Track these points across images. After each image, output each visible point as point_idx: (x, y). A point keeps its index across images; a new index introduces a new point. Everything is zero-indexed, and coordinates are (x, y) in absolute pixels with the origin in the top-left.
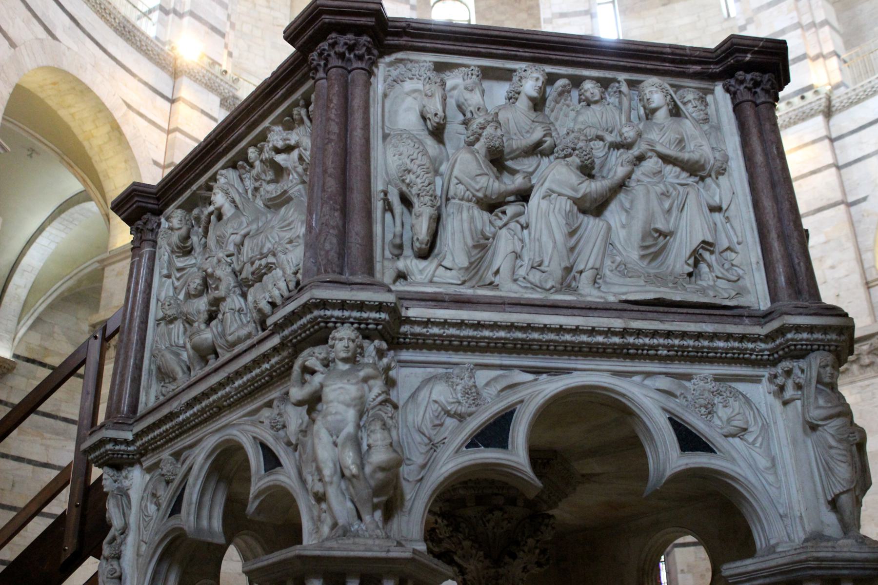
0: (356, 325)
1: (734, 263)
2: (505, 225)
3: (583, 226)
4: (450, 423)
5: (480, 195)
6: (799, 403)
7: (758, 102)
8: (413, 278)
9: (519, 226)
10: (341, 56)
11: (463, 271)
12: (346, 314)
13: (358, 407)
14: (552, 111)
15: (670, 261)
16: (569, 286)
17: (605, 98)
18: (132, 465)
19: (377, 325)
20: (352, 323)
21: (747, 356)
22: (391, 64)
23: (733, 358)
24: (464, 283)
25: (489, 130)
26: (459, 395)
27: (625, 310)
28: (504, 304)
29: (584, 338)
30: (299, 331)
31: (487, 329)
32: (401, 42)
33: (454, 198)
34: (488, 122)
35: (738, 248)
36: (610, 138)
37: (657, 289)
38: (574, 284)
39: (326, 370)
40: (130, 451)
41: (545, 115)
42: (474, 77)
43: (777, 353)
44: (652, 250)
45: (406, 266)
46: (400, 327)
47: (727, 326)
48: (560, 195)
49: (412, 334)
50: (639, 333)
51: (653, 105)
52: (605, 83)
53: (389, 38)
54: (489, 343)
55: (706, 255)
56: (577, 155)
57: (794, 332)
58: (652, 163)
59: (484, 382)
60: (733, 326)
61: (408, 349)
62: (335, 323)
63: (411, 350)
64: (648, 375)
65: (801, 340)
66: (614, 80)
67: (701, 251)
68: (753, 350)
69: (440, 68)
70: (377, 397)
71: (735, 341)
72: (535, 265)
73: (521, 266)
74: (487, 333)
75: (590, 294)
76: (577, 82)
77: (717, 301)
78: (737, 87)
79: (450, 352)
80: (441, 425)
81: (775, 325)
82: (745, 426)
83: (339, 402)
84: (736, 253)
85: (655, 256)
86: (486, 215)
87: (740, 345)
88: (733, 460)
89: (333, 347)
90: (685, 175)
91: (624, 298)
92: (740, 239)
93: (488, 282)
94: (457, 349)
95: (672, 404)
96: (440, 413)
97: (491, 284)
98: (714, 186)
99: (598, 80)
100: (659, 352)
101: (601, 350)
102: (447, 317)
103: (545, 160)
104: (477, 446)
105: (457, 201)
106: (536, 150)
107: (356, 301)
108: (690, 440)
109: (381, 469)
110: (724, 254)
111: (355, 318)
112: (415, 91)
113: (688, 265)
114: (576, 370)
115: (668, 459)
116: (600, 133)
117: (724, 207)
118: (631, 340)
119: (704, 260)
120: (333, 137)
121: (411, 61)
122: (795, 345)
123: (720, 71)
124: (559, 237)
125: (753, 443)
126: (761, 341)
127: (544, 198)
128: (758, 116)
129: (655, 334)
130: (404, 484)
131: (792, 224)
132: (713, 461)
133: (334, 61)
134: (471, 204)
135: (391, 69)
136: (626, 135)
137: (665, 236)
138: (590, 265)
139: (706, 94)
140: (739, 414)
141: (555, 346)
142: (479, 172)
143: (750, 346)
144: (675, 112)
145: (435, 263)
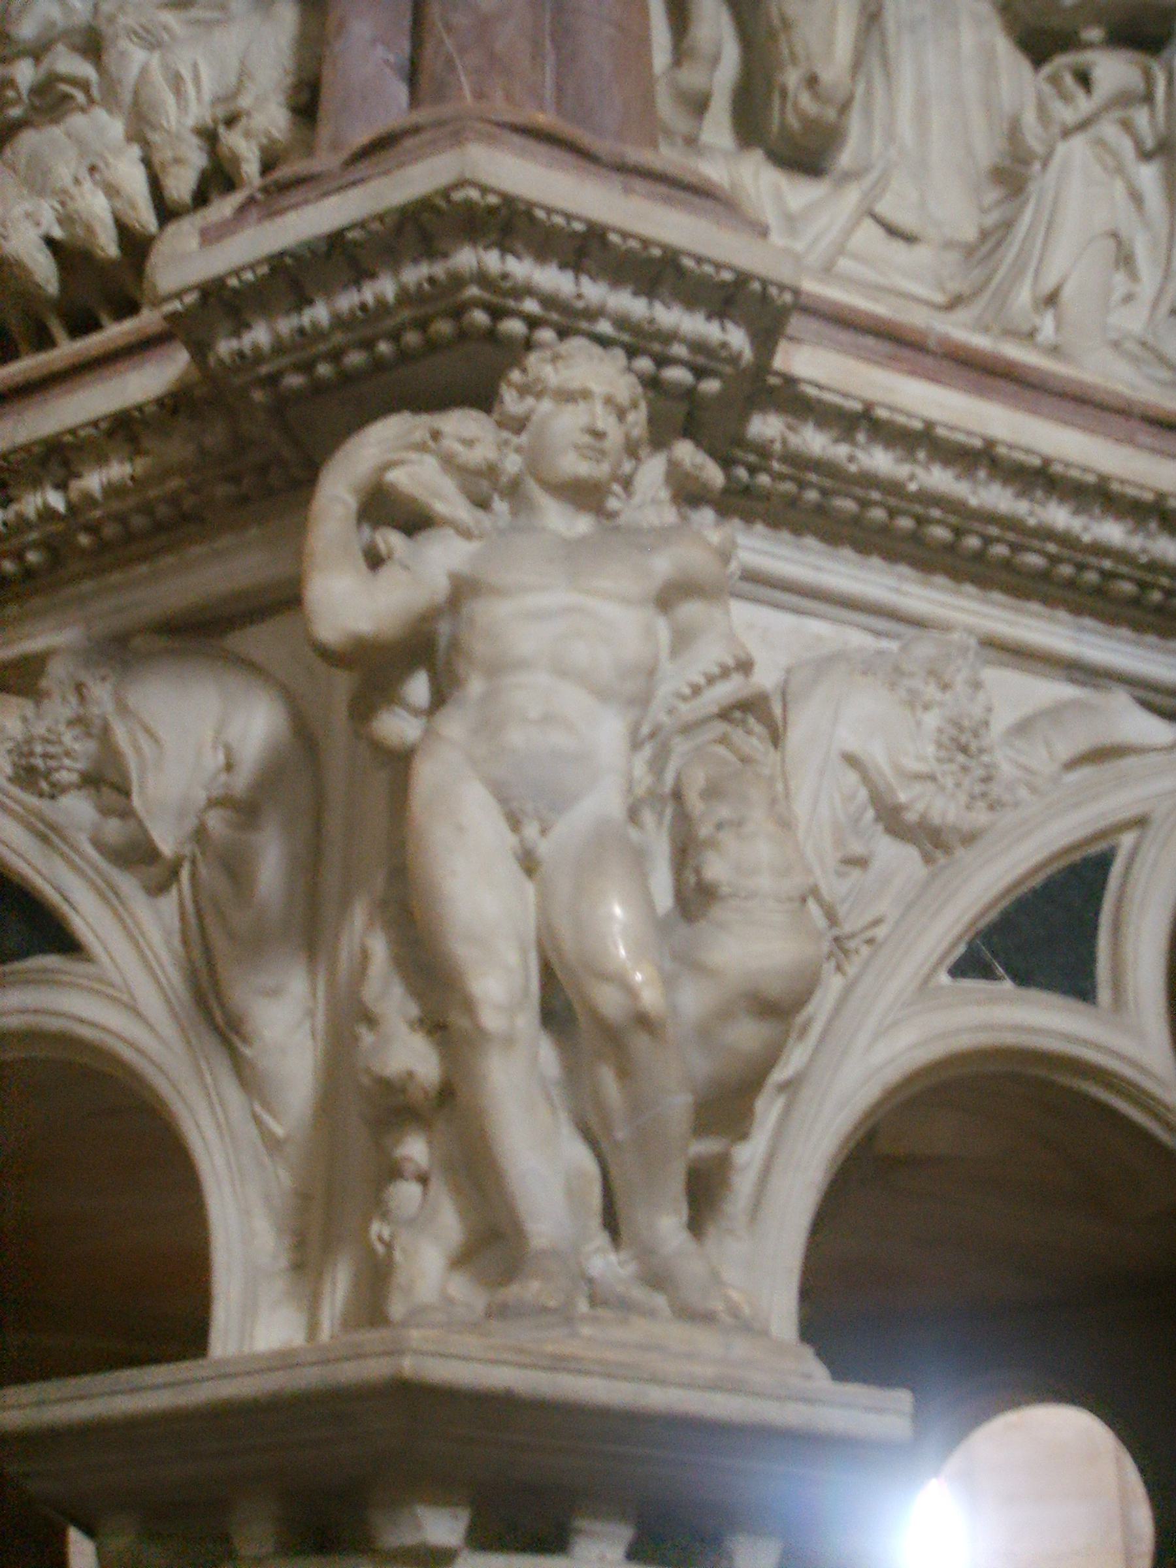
2: (1083, 125)
4: (896, 858)
9: (1127, 147)
11: (953, 257)
12: (594, 291)
19: (700, 373)
24: (954, 303)
30: (338, 338)
31: (1062, 499)
54: (1054, 560)
70: (711, 680)
73: (1128, 298)
79: (904, 569)
80: (860, 862)
83: (562, 671)
104: (986, 973)
107: (646, 243)
145: (852, 196)
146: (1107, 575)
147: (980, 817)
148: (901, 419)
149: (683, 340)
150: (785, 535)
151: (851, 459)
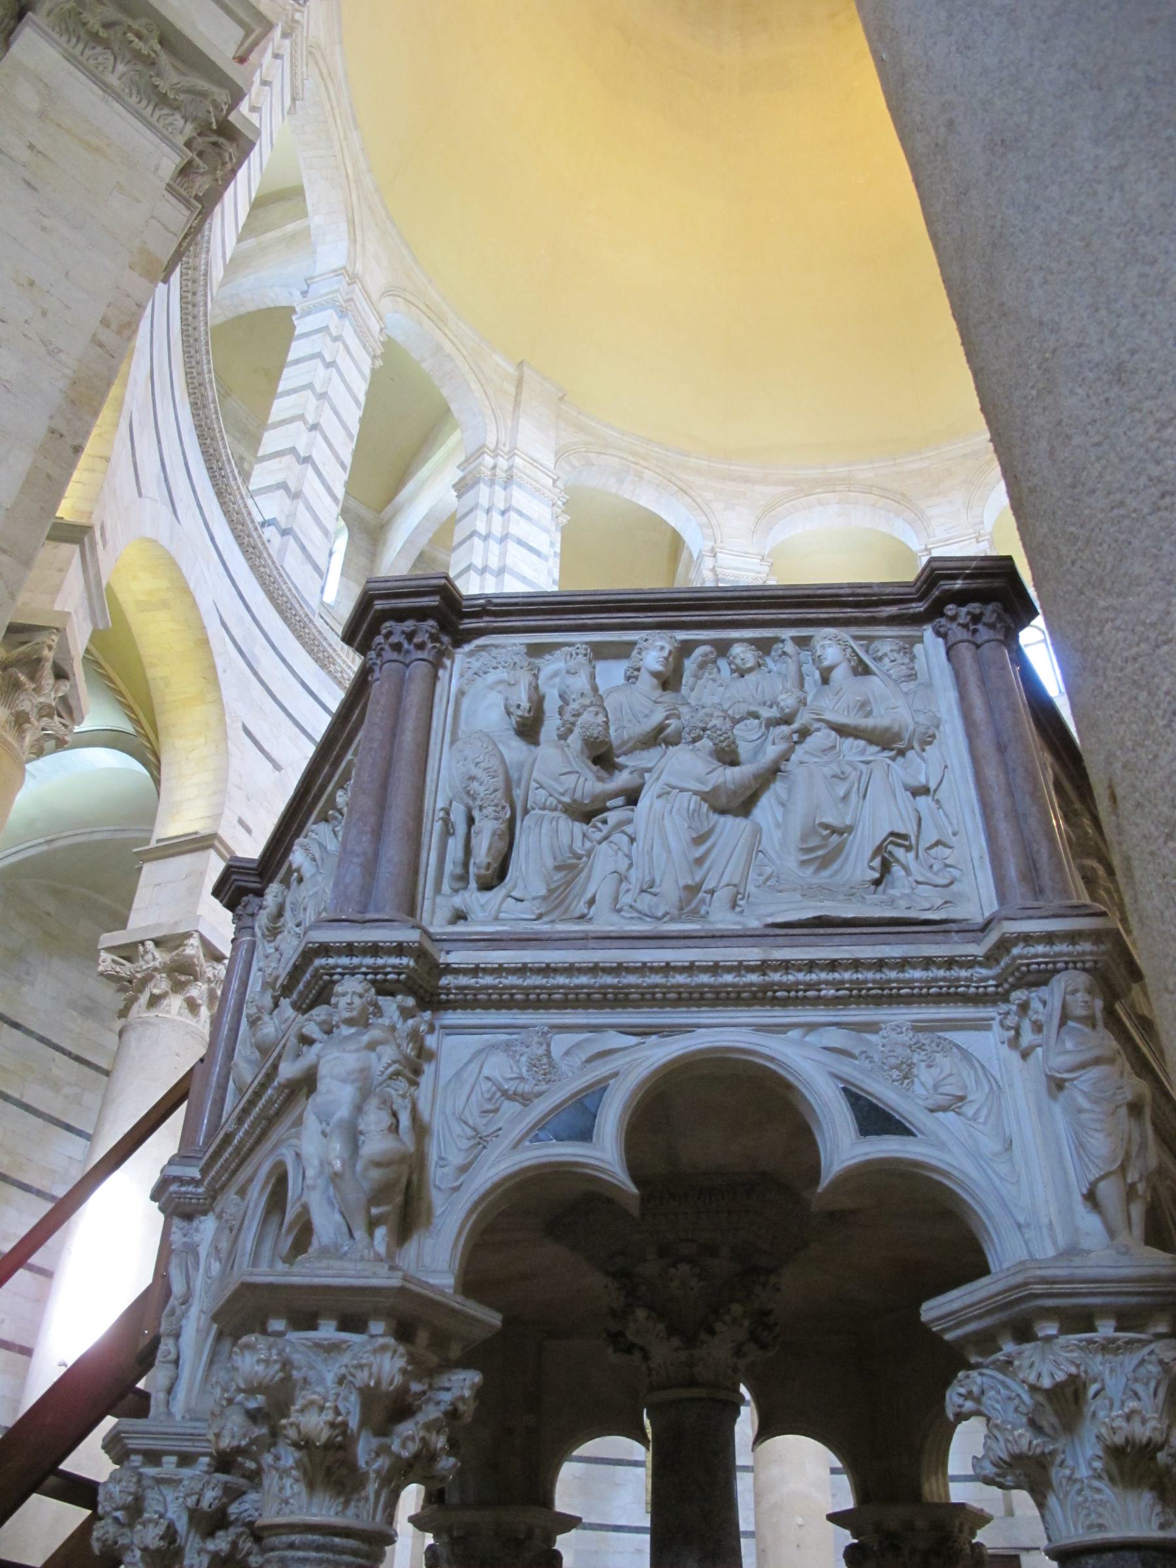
0: (370, 977)
2: (605, 838)
3: (718, 830)
4: (510, 1108)
5: (566, 799)
6: (1039, 1050)
7: (979, 642)
8: (473, 916)
9: (626, 838)
10: (397, 647)
12: (356, 961)
13: (358, 1084)
14: (692, 690)
15: (849, 867)
17: (765, 665)
18: (205, 1213)
19: (399, 974)
20: (366, 974)
21: (961, 990)
22: (471, 654)
23: (940, 995)
24: (540, 917)
25: (587, 717)
26: (524, 1070)
29: (705, 978)
33: (533, 809)
34: (585, 707)
35: (953, 841)
36: (766, 713)
39: (326, 1037)
40: (199, 1194)
41: (683, 697)
43: (1006, 980)
44: (820, 853)
45: (464, 901)
46: (439, 978)
47: (924, 947)
48: (682, 790)
49: (457, 988)
51: (826, 663)
52: (764, 647)
54: (566, 994)
55: (899, 853)
56: (708, 737)
57: (1021, 945)
58: (822, 737)
59: (564, 1050)
60: (934, 946)
61: (455, 1009)
62: (342, 975)
63: (459, 1011)
64: (811, 1027)
65: (1036, 956)
66: (777, 640)
67: (890, 847)
69: (536, 651)
71: (939, 968)
73: (628, 891)
74: (561, 980)
75: (722, 919)
76: (723, 648)
77: (912, 914)
78: (949, 626)
79: (515, 1011)
81: (993, 938)
82: (960, 1094)
85: (825, 863)
86: (578, 827)
88: (942, 1146)
89: (336, 1006)
90: (874, 749)
91: (770, 920)
92: (956, 828)
93: (578, 914)
95: (846, 1068)
96: (494, 1094)
97: (582, 917)
98: (918, 760)
100: (823, 993)
101: (733, 995)
105: (538, 812)
106: (657, 738)
107: (366, 942)
108: (874, 1118)
109: (378, 1164)
110: (932, 852)
111: (368, 967)
112: (500, 682)
113: (872, 868)
114: (699, 1026)
115: (843, 1148)
116: (752, 708)
117: (932, 786)
118: (776, 977)
119: (897, 861)
120: (375, 745)
121: (497, 646)
122: (1028, 965)
123: (926, 610)
125: (975, 1118)
126: (980, 964)
127: (659, 796)
128: (978, 660)
129: (811, 965)
130: (434, 1193)
131: (1027, 797)
132: (910, 1148)
133: (389, 654)
136: (782, 704)
137: (841, 833)
138: (724, 881)
139: (912, 645)
140: (950, 1075)
141: (664, 994)
142: (565, 770)
143: (964, 973)
144: (861, 669)
146: (589, 994)
147: (543, 1087)
150: (469, 1011)
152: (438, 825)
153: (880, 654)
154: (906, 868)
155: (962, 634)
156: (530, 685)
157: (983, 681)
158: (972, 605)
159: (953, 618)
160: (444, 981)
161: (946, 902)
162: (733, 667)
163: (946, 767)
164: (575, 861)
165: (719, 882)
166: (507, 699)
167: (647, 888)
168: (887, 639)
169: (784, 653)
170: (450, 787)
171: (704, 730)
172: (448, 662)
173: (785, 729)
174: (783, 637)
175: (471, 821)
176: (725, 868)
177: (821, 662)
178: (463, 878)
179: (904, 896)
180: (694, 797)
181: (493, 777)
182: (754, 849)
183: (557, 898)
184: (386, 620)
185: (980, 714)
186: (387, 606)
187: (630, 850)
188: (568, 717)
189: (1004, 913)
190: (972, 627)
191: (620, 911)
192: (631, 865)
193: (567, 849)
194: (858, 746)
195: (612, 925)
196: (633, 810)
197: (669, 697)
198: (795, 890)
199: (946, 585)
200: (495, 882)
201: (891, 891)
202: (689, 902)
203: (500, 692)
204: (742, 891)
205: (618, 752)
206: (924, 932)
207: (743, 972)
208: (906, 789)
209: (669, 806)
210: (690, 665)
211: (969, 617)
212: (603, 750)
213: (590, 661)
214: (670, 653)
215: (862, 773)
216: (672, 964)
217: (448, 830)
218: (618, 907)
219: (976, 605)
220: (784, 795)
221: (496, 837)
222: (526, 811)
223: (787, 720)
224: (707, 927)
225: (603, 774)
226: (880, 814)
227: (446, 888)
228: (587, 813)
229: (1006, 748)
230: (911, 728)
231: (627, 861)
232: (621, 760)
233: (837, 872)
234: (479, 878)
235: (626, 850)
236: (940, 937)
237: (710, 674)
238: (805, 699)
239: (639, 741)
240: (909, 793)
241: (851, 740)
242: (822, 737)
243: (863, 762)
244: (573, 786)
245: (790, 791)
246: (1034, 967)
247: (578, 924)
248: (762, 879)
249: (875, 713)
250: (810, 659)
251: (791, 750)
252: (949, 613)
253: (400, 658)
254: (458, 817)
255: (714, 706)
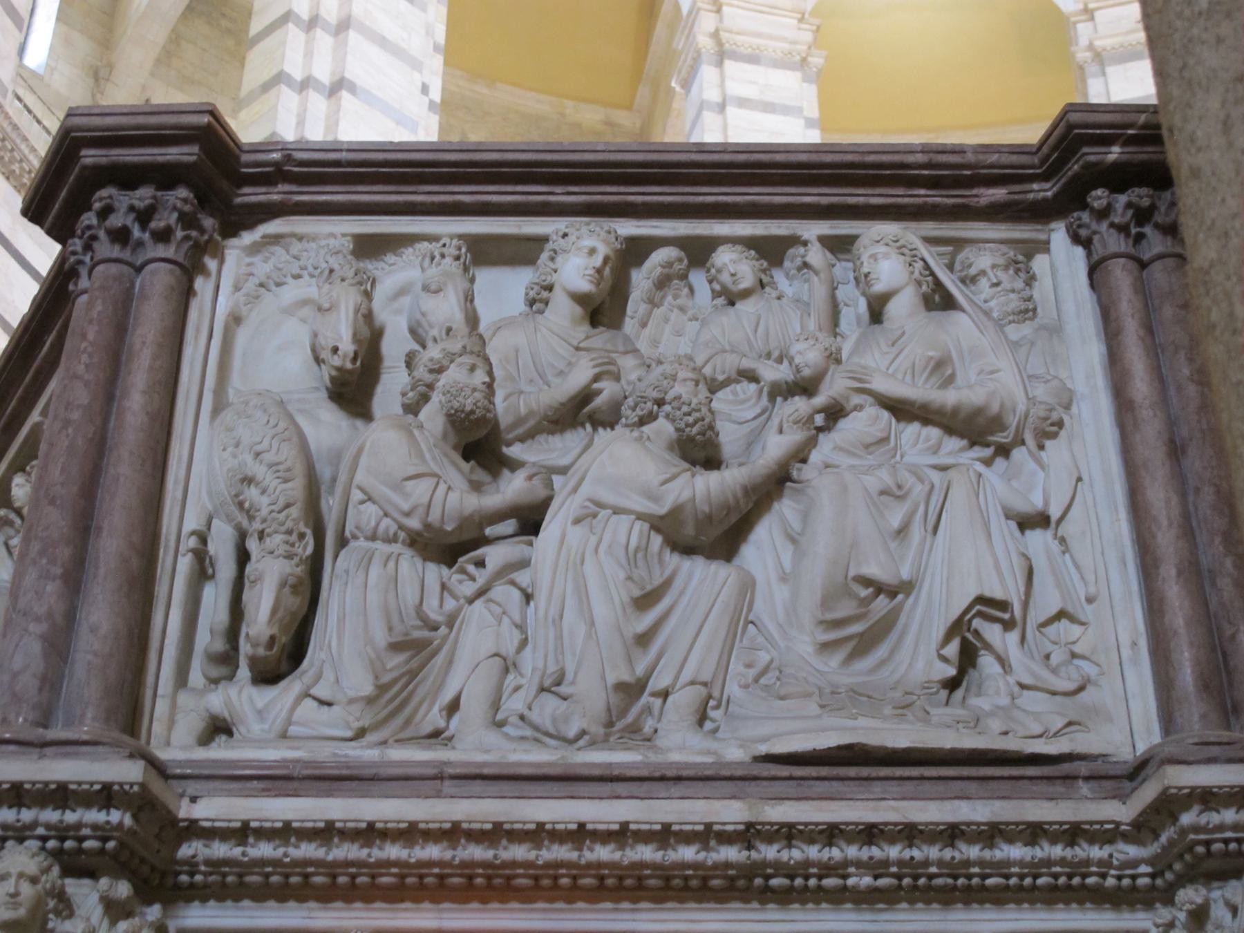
0: (51, 844)
1: (1077, 649)
2: (481, 593)
3: (678, 583)
5: (414, 523)
7: (1146, 257)
8: (242, 729)
9: (516, 595)
10: (121, 236)
11: (356, 709)
12: (27, 815)
14: (644, 325)
15: (905, 653)
16: (634, 729)
17: (773, 285)
19: (105, 840)
20: (44, 839)
21: (1091, 880)
22: (255, 249)
23: (1054, 888)
24: (361, 733)
25: (455, 374)
27: (755, 778)
28: (440, 777)
29: (646, 853)
31: (394, 841)
32: (275, 197)
33: (355, 537)
34: (452, 357)
36: (772, 373)
37: (850, 723)
38: (648, 725)
41: (627, 339)
42: (448, 260)
43: (1170, 867)
45: (228, 703)
46: (179, 846)
48: (617, 511)
49: (208, 862)
50: (789, 833)
52: (771, 252)
53: (246, 190)
54: (402, 877)
55: (992, 632)
56: (667, 416)
57: (1196, 808)
58: (865, 422)
60: (1046, 804)
61: (204, 900)
63: (212, 903)
65: (1221, 828)
66: (795, 241)
67: (977, 623)
68: (1106, 863)
69: (369, 247)
71: (1054, 842)
72: (547, 683)
73: (517, 689)
74: (394, 851)
75: (680, 745)
76: (698, 252)
77: (1012, 744)
78: (1094, 226)
79: (312, 904)
81: (1147, 793)
84: (1083, 624)
85: (864, 644)
86: (434, 573)
87: (1068, 853)
90: (954, 443)
91: (763, 749)
92: (1092, 590)
93: (427, 728)
94: (327, 895)
97: (436, 734)
98: (1032, 465)
99: (752, 243)
100: (851, 882)
101: (694, 883)
102: (289, 816)
103: (603, 434)
105: (362, 543)
106: (579, 413)
107: (47, 784)
110: (1051, 630)
111: (48, 826)
112: (305, 302)
113: (944, 659)
116: (746, 364)
117: (1055, 513)
118: (769, 852)
119: (988, 647)
120: (76, 415)
121: (300, 238)
122: (1208, 843)
123: (1056, 196)
124: (602, 611)
126: (1127, 838)
127: (577, 521)
128: (1142, 290)
129: (831, 833)
131: (1218, 540)
133: (104, 248)
134: (396, 548)
135: (257, 259)
136: (797, 360)
137: (892, 594)
139: (1029, 256)
141: (575, 878)
142: (412, 471)
143: (1097, 852)
144: (939, 300)
146: (441, 877)
148: (268, 825)
149: (86, 826)
150: (229, 903)
151: (244, 854)
152: (185, 564)
153: (973, 271)
154: (1002, 661)
155: (1115, 243)
156: (357, 311)
157: (1149, 328)
158: (1137, 190)
159: (1103, 214)
160: (185, 851)
161: (1070, 724)
162: (717, 287)
163: (1079, 479)
164: (426, 634)
165: (677, 677)
166: (315, 335)
167: (553, 686)
168: (986, 249)
169: (806, 265)
170: (210, 493)
171: (660, 403)
172: (211, 264)
173: (800, 405)
174: (806, 236)
175: (243, 557)
176: (686, 653)
177: (868, 285)
178: (227, 659)
179: (997, 710)
180: (638, 524)
181: (286, 481)
182: (741, 618)
183: (392, 700)
184: (102, 186)
185: (1141, 387)
186: (104, 160)
187: (524, 617)
188: (421, 372)
189: (1170, 750)
190: (1134, 231)
191: (500, 725)
192: (524, 643)
193: (413, 613)
194: (927, 439)
195: (487, 751)
196: (531, 544)
197: (601, 338)
198: (808, 695)
199: (1092, 154)
200: (284, 666)
201: (974, 701)
202: (624, 712)
203: (304, 321)
204: (716, 694)
205: (510, 436)
206: (1031, 778)
207: (713, 843)
208: (1008, 517)
209: (593, 540)
210: (641, 279)
211: (1130, 213)
212: (481, 433)
213: (466, 269)
214: (606, 260)
215: (933, 486)
216: (589, 827)
217: (203, 570)
218: (499, 717)
219: (1144, 191)
220: (796, 525)
221: (287, 590)
222: (342, 542)
223: (805, 387)
224: (653, 758)
225: (481, 475)
226: (962, 562)
227: (196, 677)
228: (450, 546)
229: (1184, 452)
230: (1021, 407)
231: (517, 636)
232: (514, 451)
233: (882, 663)
234: (254, 662)
235: (517, 618)
236: (1059, 788)
237: (676, 297)
238: (839, 350)
239: (546, 418)
240: (1013, 525)
241: (915, 427)
242: (865, 422)
243: (935, 467)
244: (425, 500)
245: (805, 517)
246: (1217, 847)
247: (429, 748)
248: (752, 673)
249: (959, 380)
250: (851, 275)
251: (811, 443)
252: (1096, 204)
253: (126, 255)
254: (222, 549)
255: (679, 360)
